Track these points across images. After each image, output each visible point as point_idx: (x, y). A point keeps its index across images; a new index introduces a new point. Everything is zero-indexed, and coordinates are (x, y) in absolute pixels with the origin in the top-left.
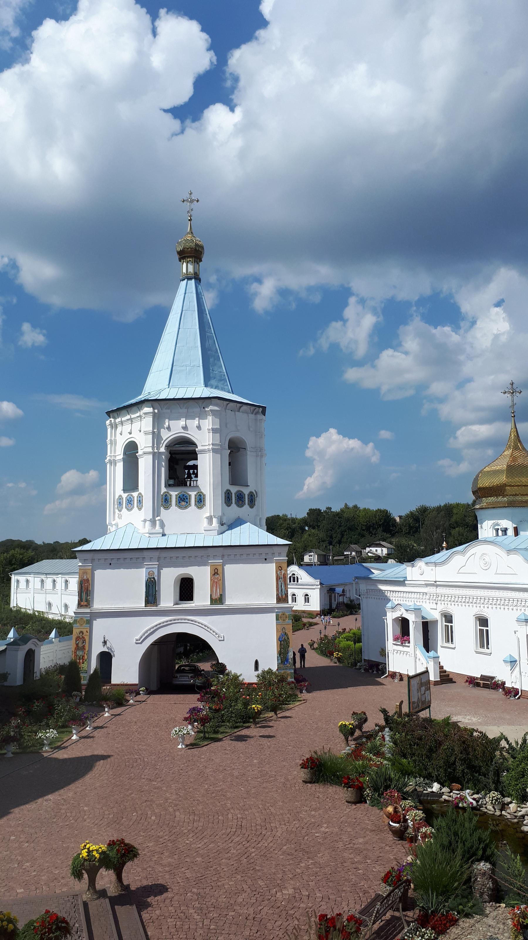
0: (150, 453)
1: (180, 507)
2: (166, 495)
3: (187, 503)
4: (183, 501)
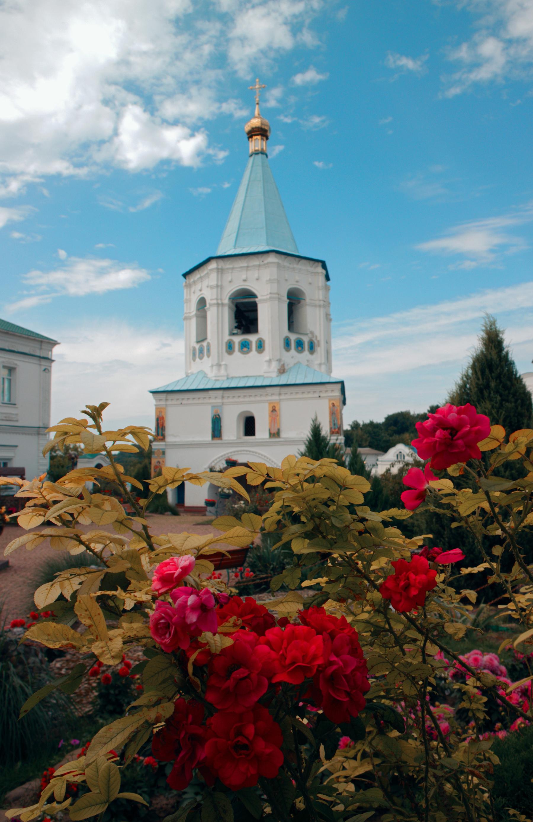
0: (214, 304)
4: (245, 346)
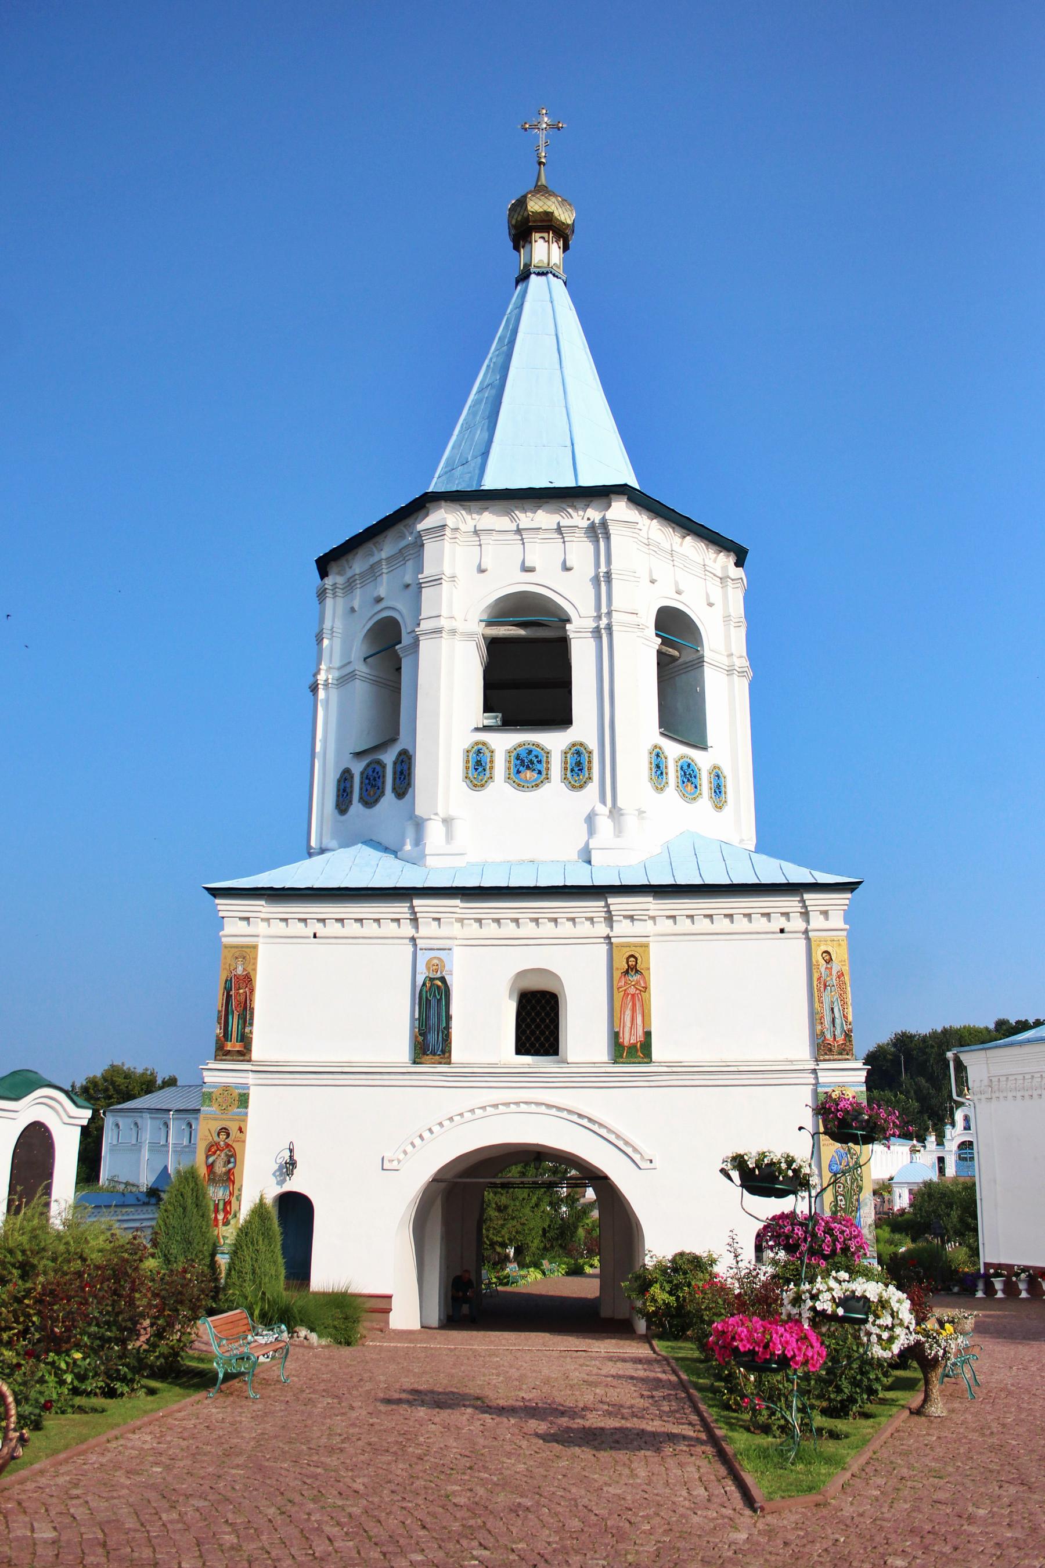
1: (520, 786)
2: (479, 752)
3: (540, 772)
4: (528, 766)
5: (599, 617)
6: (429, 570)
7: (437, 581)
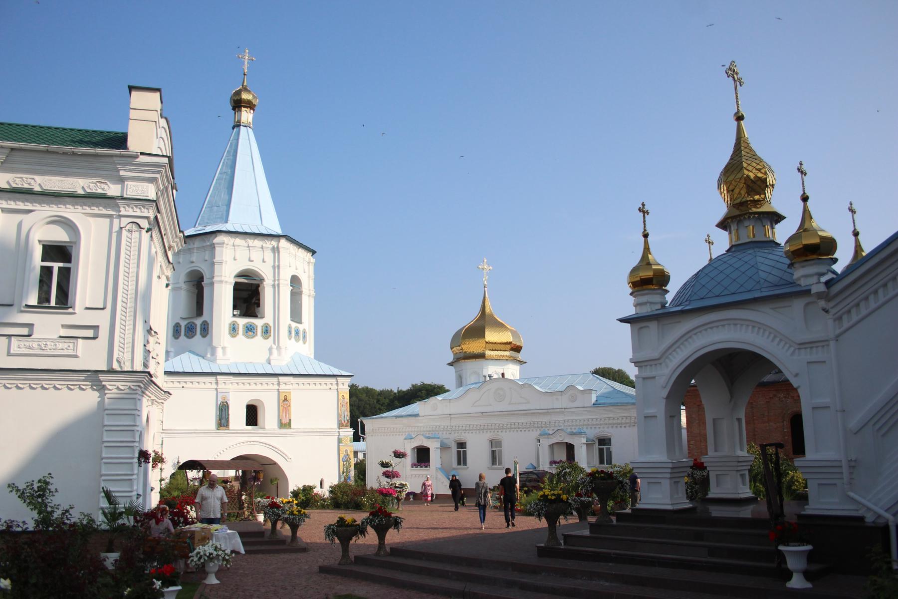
1: (247, 337)
4: (250, 330)
5: (274, 281)
6: (217, 259)
7: (221, 263)
